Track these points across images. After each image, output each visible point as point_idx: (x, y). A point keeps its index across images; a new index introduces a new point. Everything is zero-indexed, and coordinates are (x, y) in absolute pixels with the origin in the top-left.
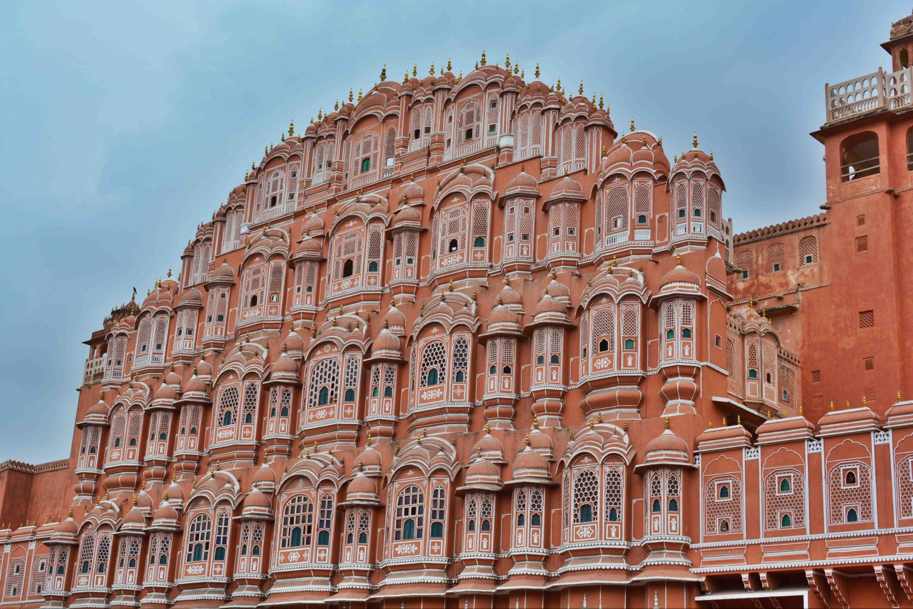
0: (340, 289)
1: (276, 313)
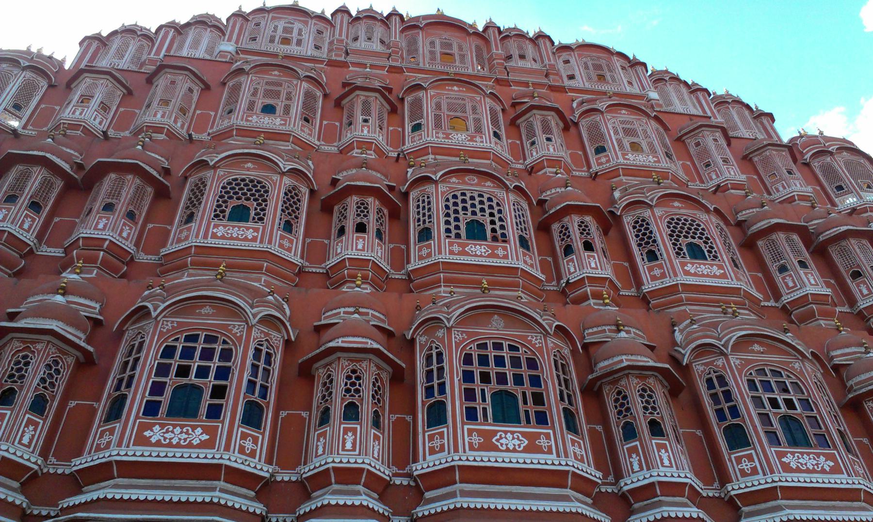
0: (447, 138)
1: (310, 135)
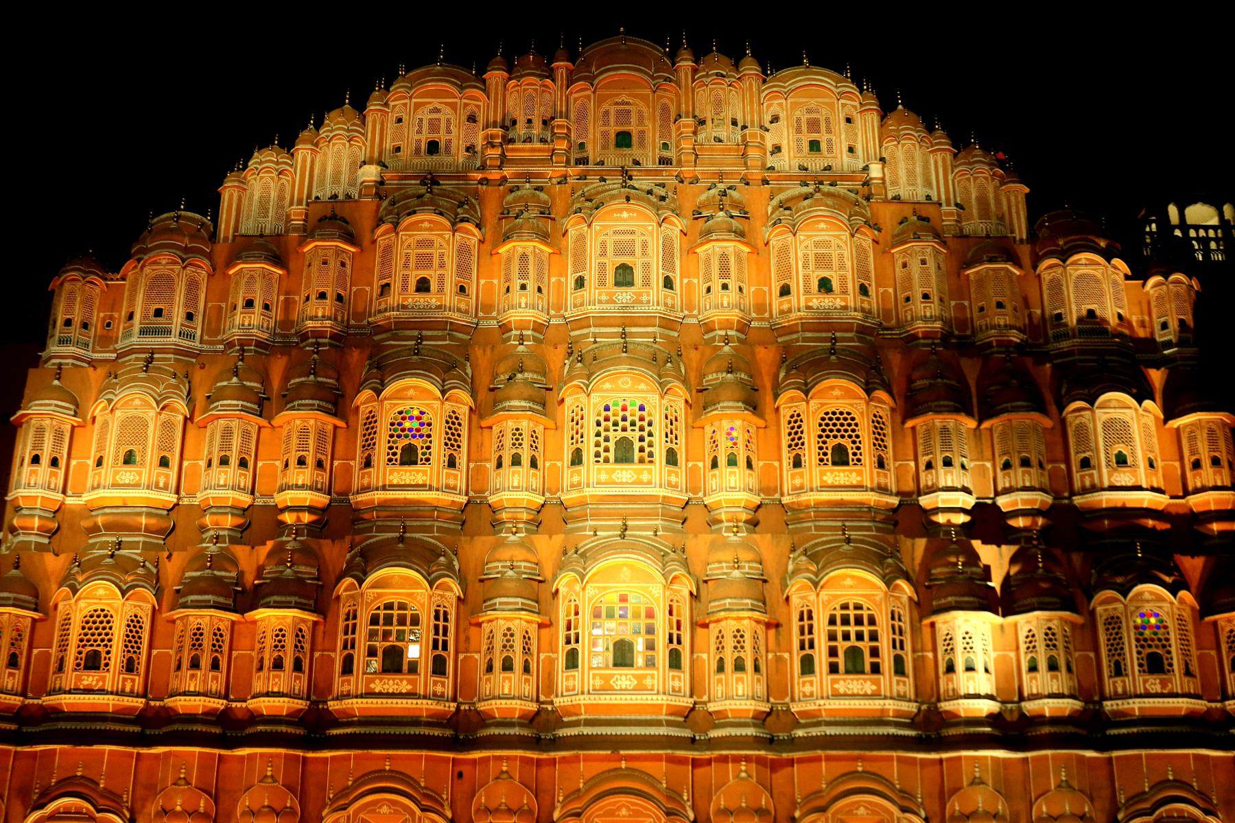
0: (611, 301)
